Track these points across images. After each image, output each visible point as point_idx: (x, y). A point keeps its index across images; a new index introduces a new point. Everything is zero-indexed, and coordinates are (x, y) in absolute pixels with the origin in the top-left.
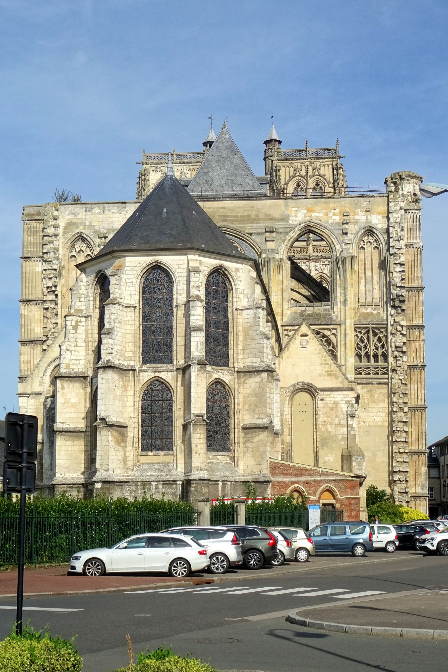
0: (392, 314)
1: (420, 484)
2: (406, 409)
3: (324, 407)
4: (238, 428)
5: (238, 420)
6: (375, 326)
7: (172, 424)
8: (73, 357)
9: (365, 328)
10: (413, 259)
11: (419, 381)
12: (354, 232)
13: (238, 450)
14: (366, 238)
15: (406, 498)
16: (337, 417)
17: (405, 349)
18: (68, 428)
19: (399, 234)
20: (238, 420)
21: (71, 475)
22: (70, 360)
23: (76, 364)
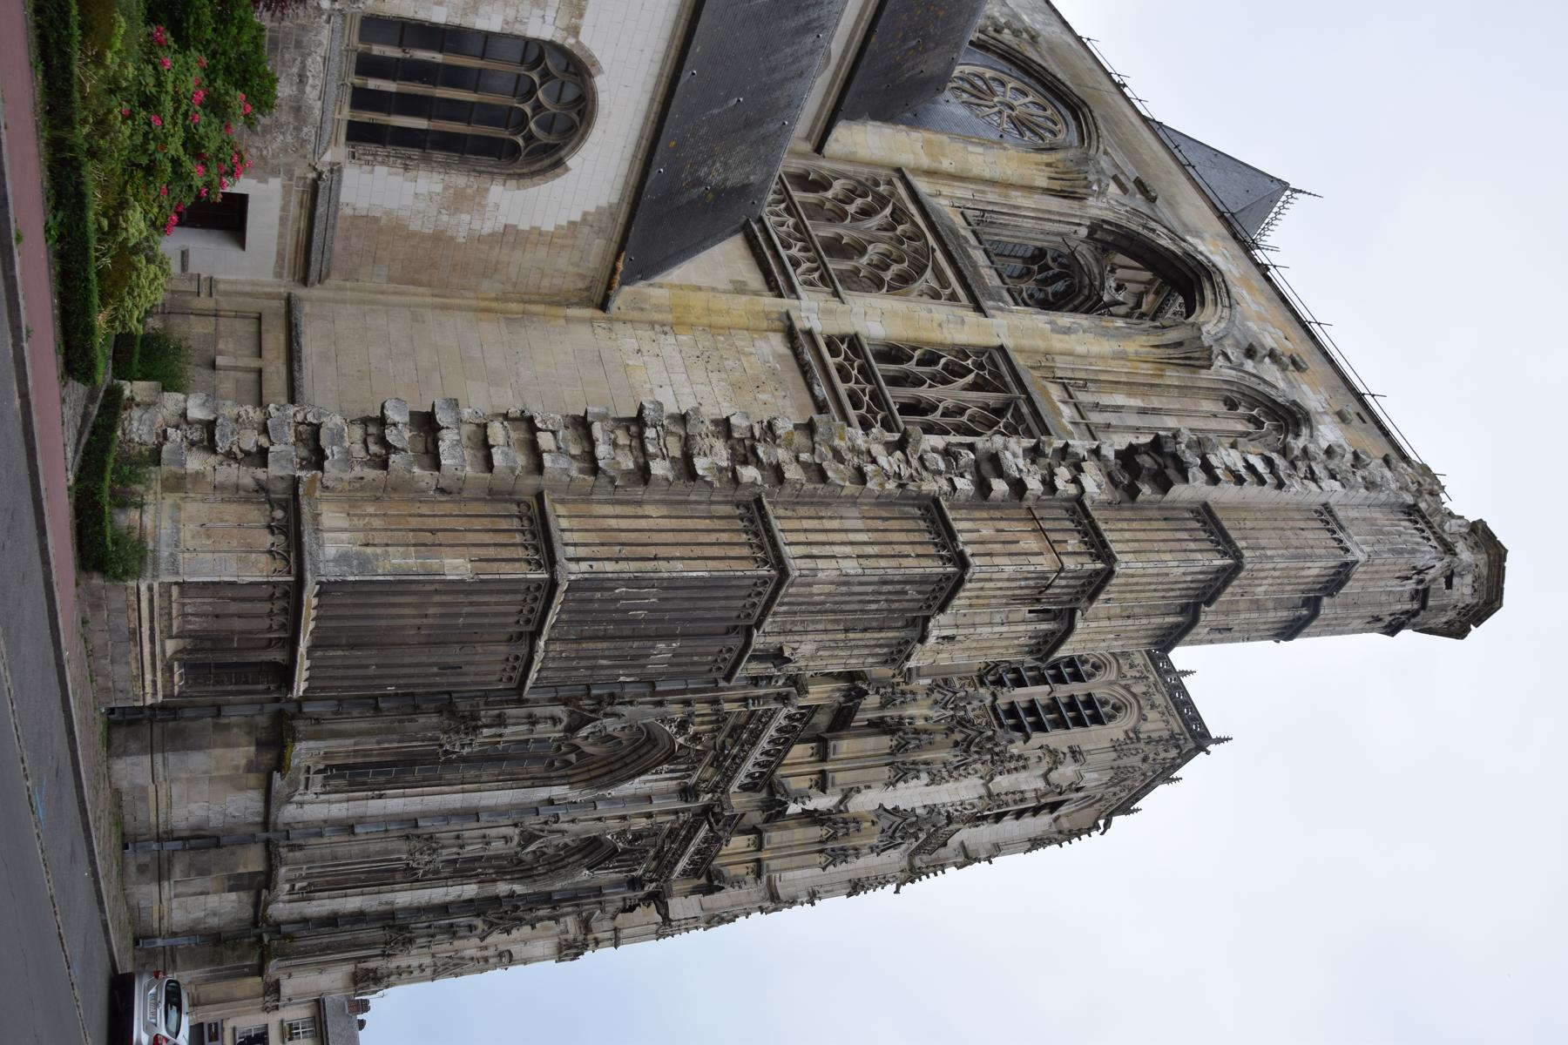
0: (1104, 451)
1: (369, 550)
2: (749, 473)
6: (1025, 410)
11: (888, 550)
15: (284, 461)
17: (999, 487)
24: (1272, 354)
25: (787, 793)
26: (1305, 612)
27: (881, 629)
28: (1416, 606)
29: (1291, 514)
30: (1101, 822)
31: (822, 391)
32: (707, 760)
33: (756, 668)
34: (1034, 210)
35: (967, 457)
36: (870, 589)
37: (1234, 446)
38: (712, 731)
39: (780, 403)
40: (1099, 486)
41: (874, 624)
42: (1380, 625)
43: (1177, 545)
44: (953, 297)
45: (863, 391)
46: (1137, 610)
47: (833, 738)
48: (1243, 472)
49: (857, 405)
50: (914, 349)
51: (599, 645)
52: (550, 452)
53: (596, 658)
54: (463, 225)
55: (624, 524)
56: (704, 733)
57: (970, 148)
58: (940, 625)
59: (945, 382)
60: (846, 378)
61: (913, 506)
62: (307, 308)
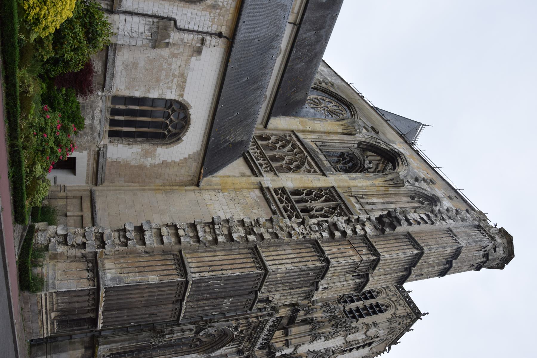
1: (122, 275)
2: (252, 238)
6: (343, 207)
11: (302, 260)
17: (337, 234)
24: (424, 179)
25: (275, 349)
26: (447, 266)
27: (302, 287)
28: (485, 260)
29: (438, 233)
30: (387, 348)
31: (274, 207)
32: (246, 339)
33: (260, 305)
34: (339, 140)
36: (297, 274)
37: (415, 212)
38: (247, 329)
39: (260, 212)
40: (371, 230)
41: (300, 286)
42: (474, 267)
43: (400, 248)
44: (315, 172)
45: (288, 206)
46: (390, 272)
47: (289, 328)
48: (419, 220)
49: (286, 211)
50: (304, 190)
51: (205, 302)
52: (183, 236)
53: (204, 307)
54: (149, 162)
55: (210, 259)
56: (244, 330)
57: (315, 122)
58: (322, 284)
59: (315, 200)
60: (282, 202)
61: (309, 243)
62: (97, 193)
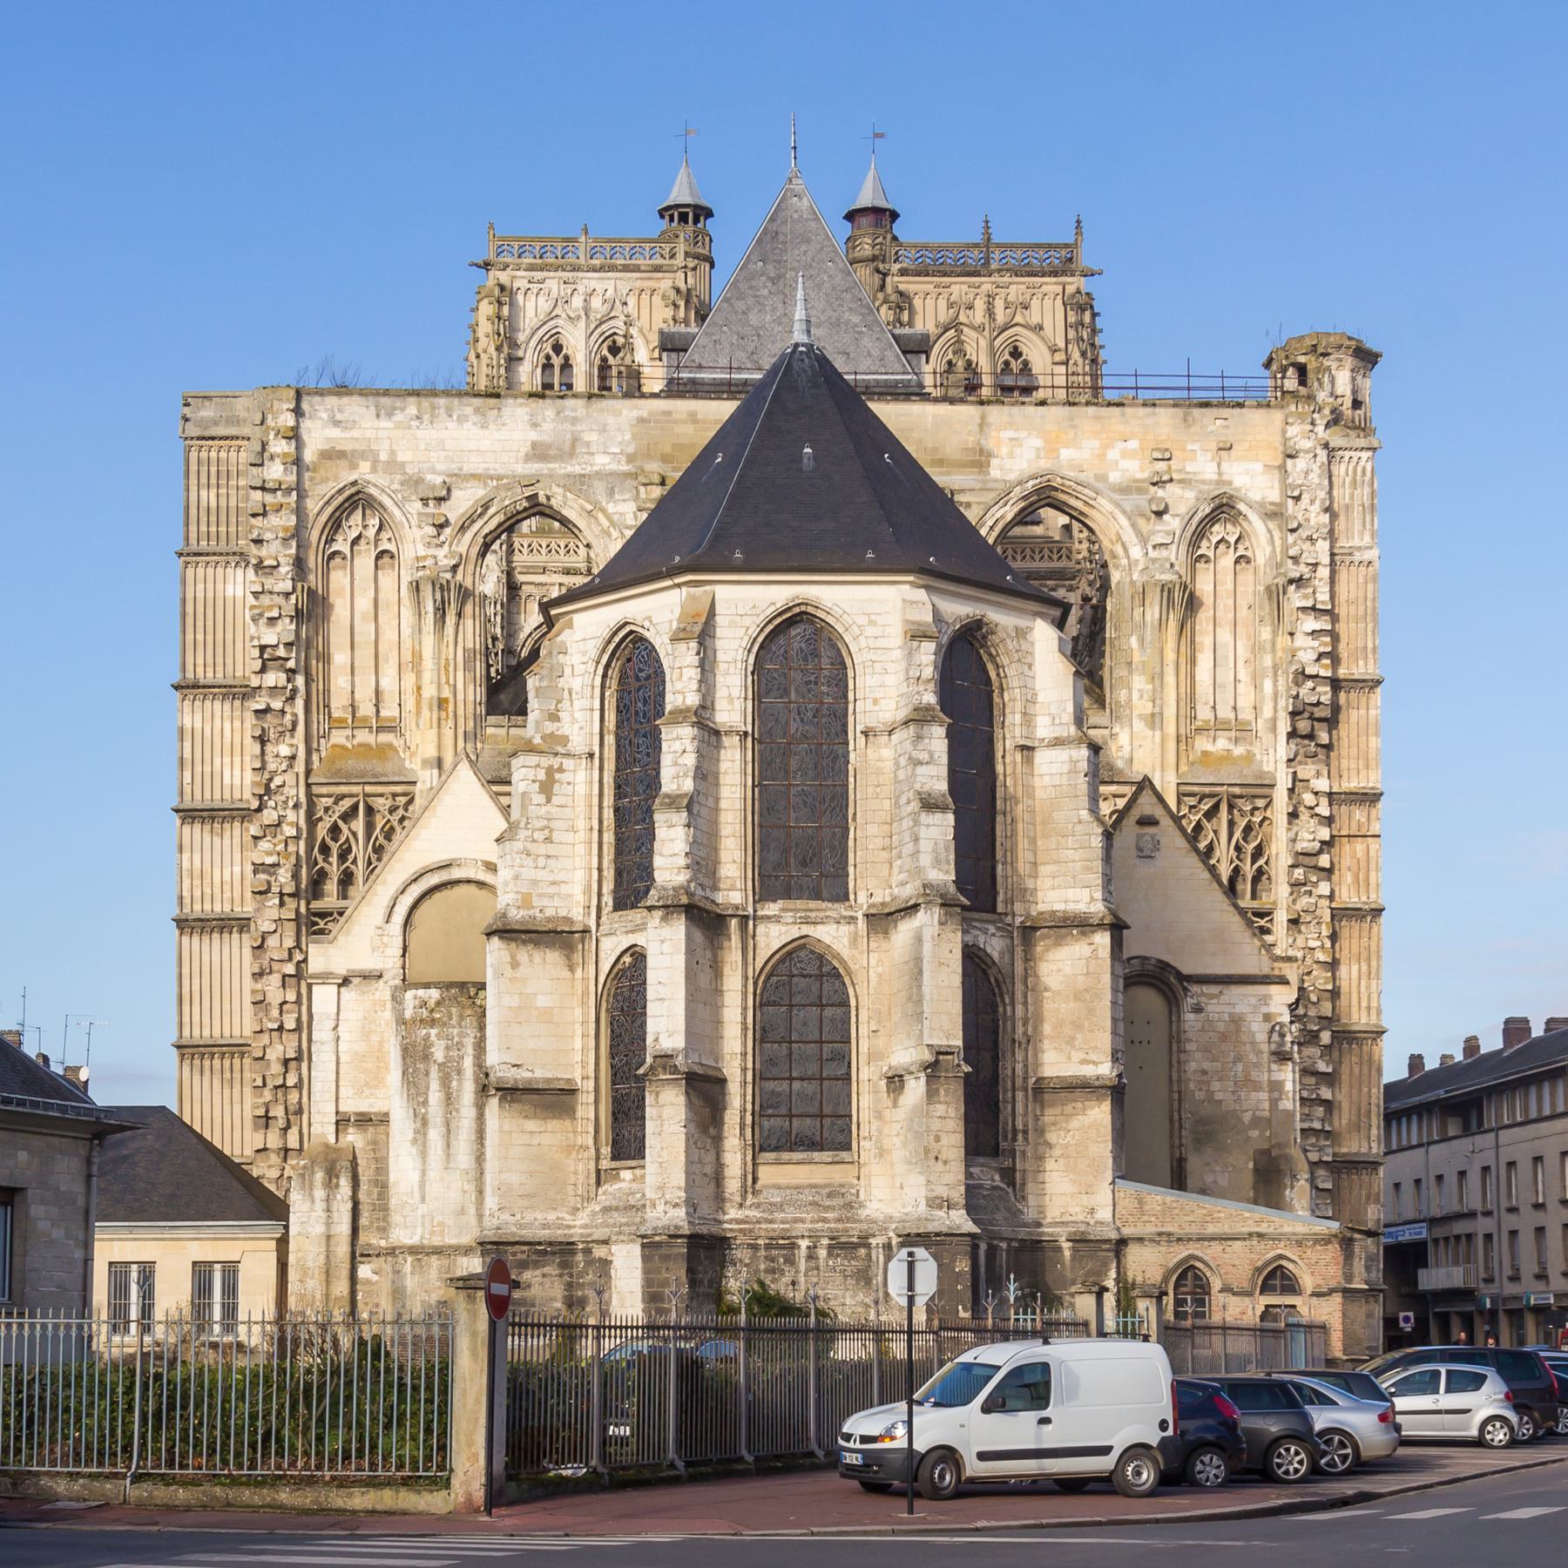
2: (1326, 1037)
3: (1203, 1030)
4: (1026, 1090)
5: (1026, 1066)
7: (849, 1074)
8: (541, 875)
9: (1212, 796)
10: (1352, 596)
11: (1364, 954)
12: (1183, 510)
13: (1024, 1152)
14: (1216, 528)
16: (1238, 1059)
17: (1324, 861)
18: (530, 1080)
19: (1312, 523)
20: (1026, 1066)
21: (539, 1216)
22: (534, 882)
23: (551, 896)
35: (1299, 873)
